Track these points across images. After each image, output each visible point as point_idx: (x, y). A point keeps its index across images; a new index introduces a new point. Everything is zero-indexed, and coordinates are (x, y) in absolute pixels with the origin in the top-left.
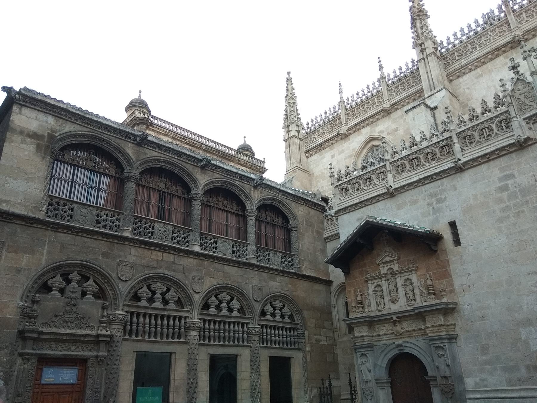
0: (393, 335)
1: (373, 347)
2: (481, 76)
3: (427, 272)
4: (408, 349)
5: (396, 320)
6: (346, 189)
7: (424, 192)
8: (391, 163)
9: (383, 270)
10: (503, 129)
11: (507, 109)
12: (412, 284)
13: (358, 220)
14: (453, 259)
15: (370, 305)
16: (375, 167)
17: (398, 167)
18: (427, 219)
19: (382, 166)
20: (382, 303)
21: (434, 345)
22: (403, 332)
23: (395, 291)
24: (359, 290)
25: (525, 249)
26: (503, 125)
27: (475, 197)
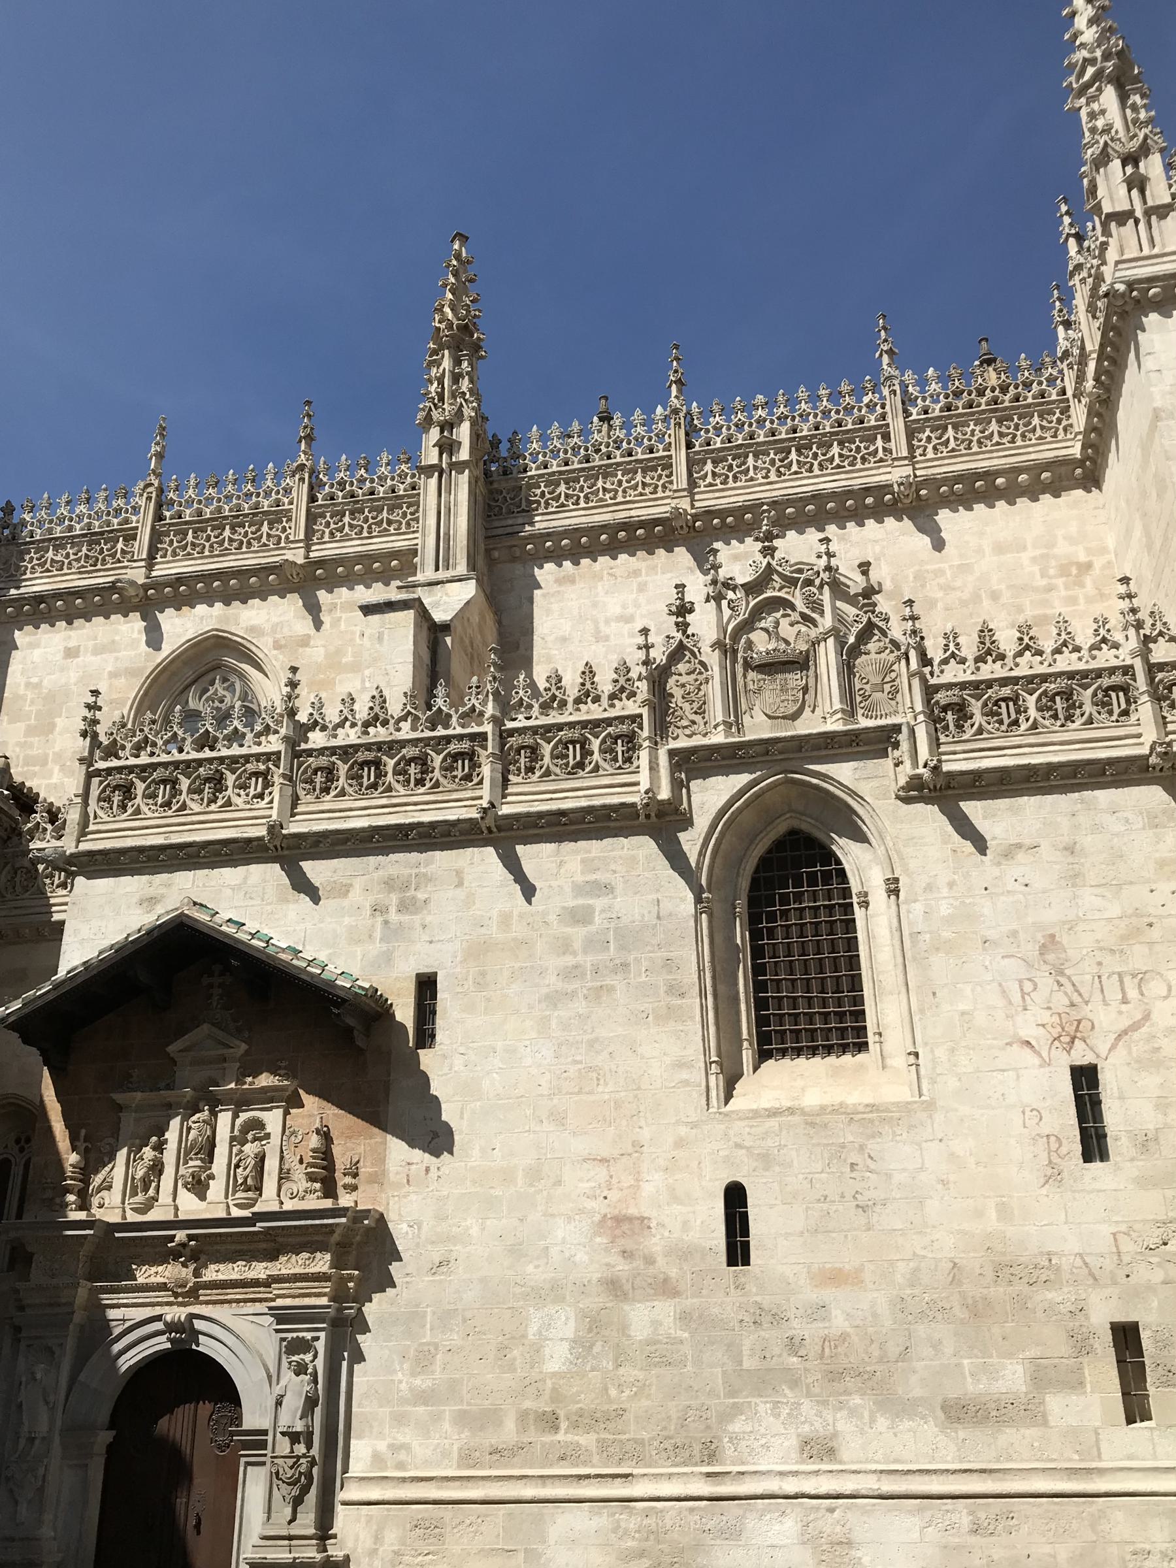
2: (571, 580)
6: (127, 791)
7: (371, 869)
10: (615, 760)
11: (638, 711)
16: (244, 751)
18: (359, 951)
24: (83, 1132)
25: (590, 1093)
26: (619, 749)
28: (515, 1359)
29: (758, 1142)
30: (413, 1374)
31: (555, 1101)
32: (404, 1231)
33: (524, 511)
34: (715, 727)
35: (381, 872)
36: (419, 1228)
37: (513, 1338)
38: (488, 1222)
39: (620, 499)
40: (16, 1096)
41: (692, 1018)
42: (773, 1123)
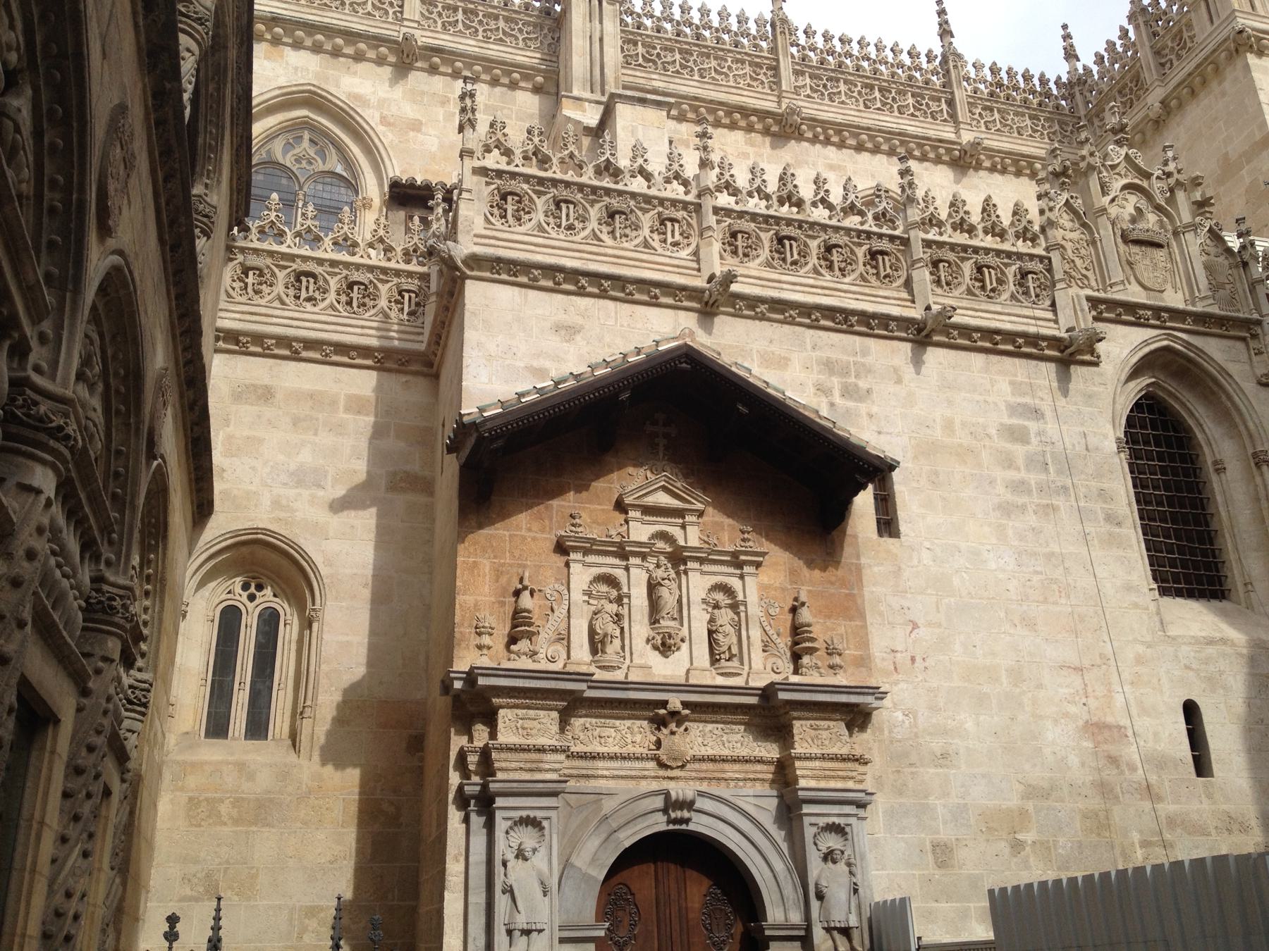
0: (652, 764)
3: (792, 582)
5: (674, 714)
7: (809, 347)
8: (716, 210)
10: (1026, 293)
11: (1044, 253)
13: (558, 328)
14: (876, 569)
15: (565, 638)
16: (653, 192)
17: (734, 235)
19: (685, 205)
20: (617, 642)
21: (813, 820)
22: (695, 759)
25: (1055, 603)
27: (949, 426)
29: (1203, 666)
33: (640, 65)
34: (1111, 286)
35: (818, 353)
36: (915, 718)
38: (982, 718)
39: (731, 83)
40: (265, 531)
41: (1131, 546)
42: (1211, 650)
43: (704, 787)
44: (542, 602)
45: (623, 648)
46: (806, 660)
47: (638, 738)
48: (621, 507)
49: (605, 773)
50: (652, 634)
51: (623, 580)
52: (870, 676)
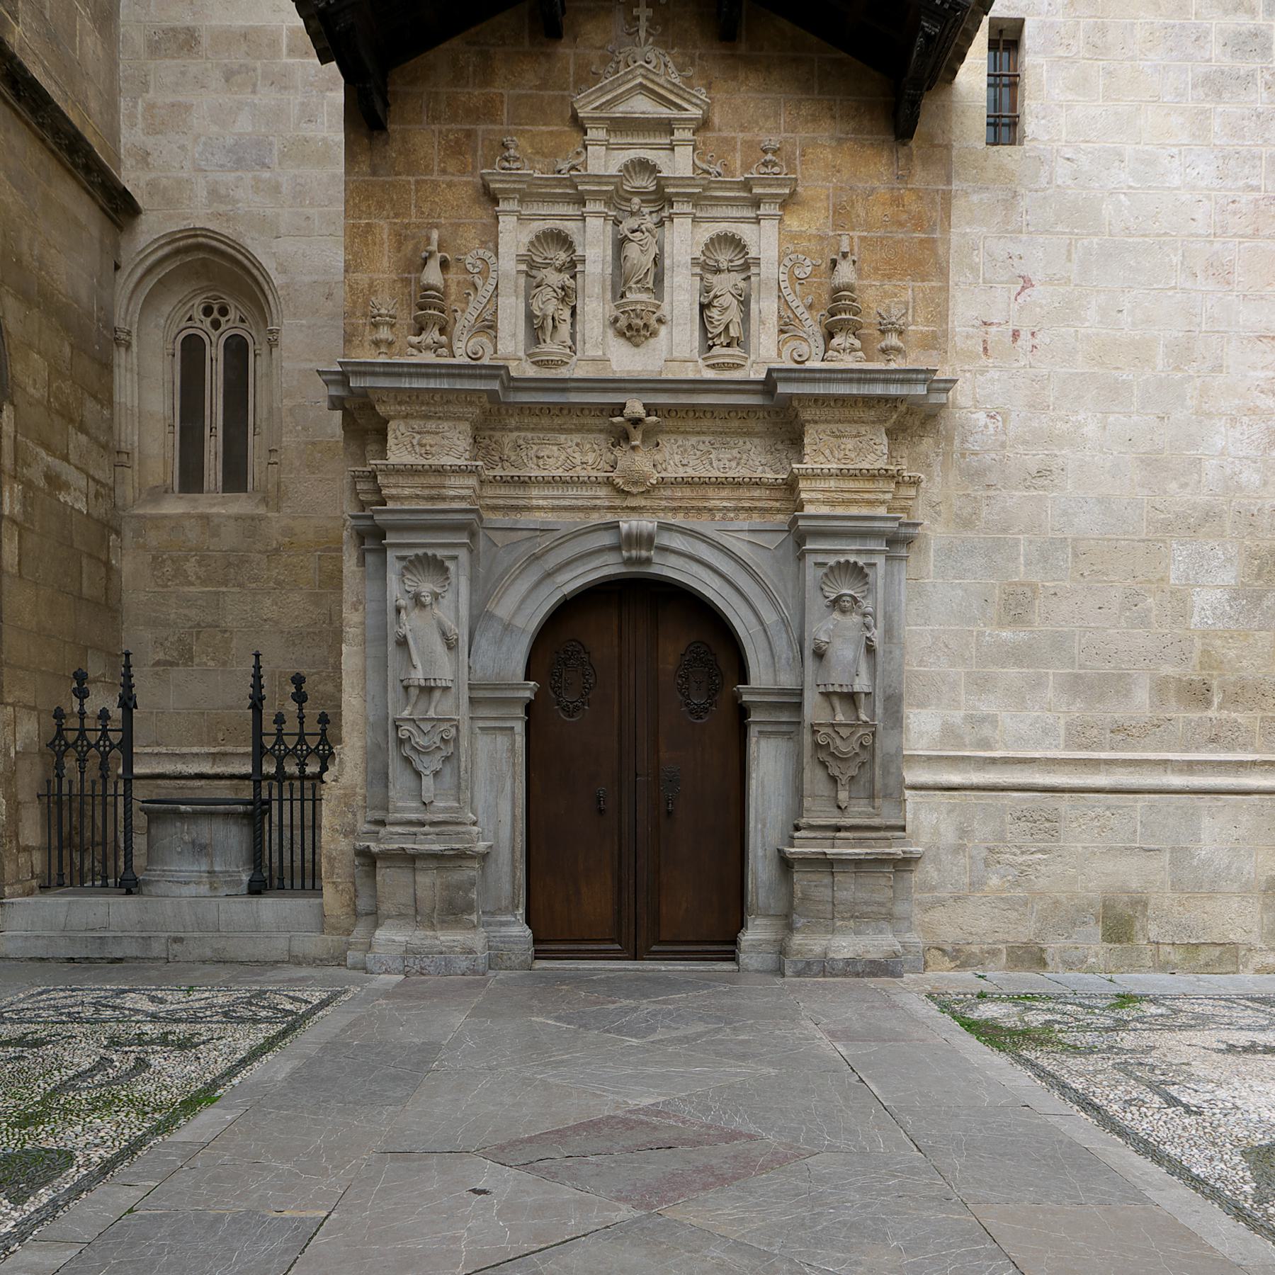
0: (602, 492)
1: (473, 535)
3: (836, 226)
4: (673, 560)
5: (636, 422)
9: (604, 160)
12: (746, 267)
14: (975, 198)
15: (489, 327)
20: (565, 329)
23: (650, 285)
24: (435, 235)
28: (1150, 610)
30: (1001, 625)
31: (1217, 246)
32: (982, 423)
36: (1004, 421)
37: (1150, 581)
38: (1111, 418)
43: (678, 520)
44: (461, 277)
45: (573, 336)
46: (835, 342)
47: (590, 458)
48: (579, 125)
49: (541, 502)
50: (616, 313)
51: (576, 238)
52: (944, 361)
